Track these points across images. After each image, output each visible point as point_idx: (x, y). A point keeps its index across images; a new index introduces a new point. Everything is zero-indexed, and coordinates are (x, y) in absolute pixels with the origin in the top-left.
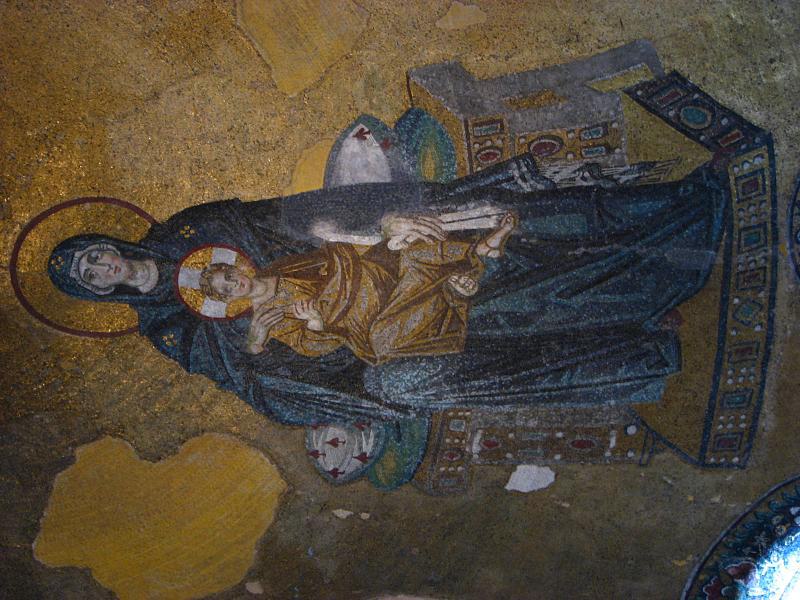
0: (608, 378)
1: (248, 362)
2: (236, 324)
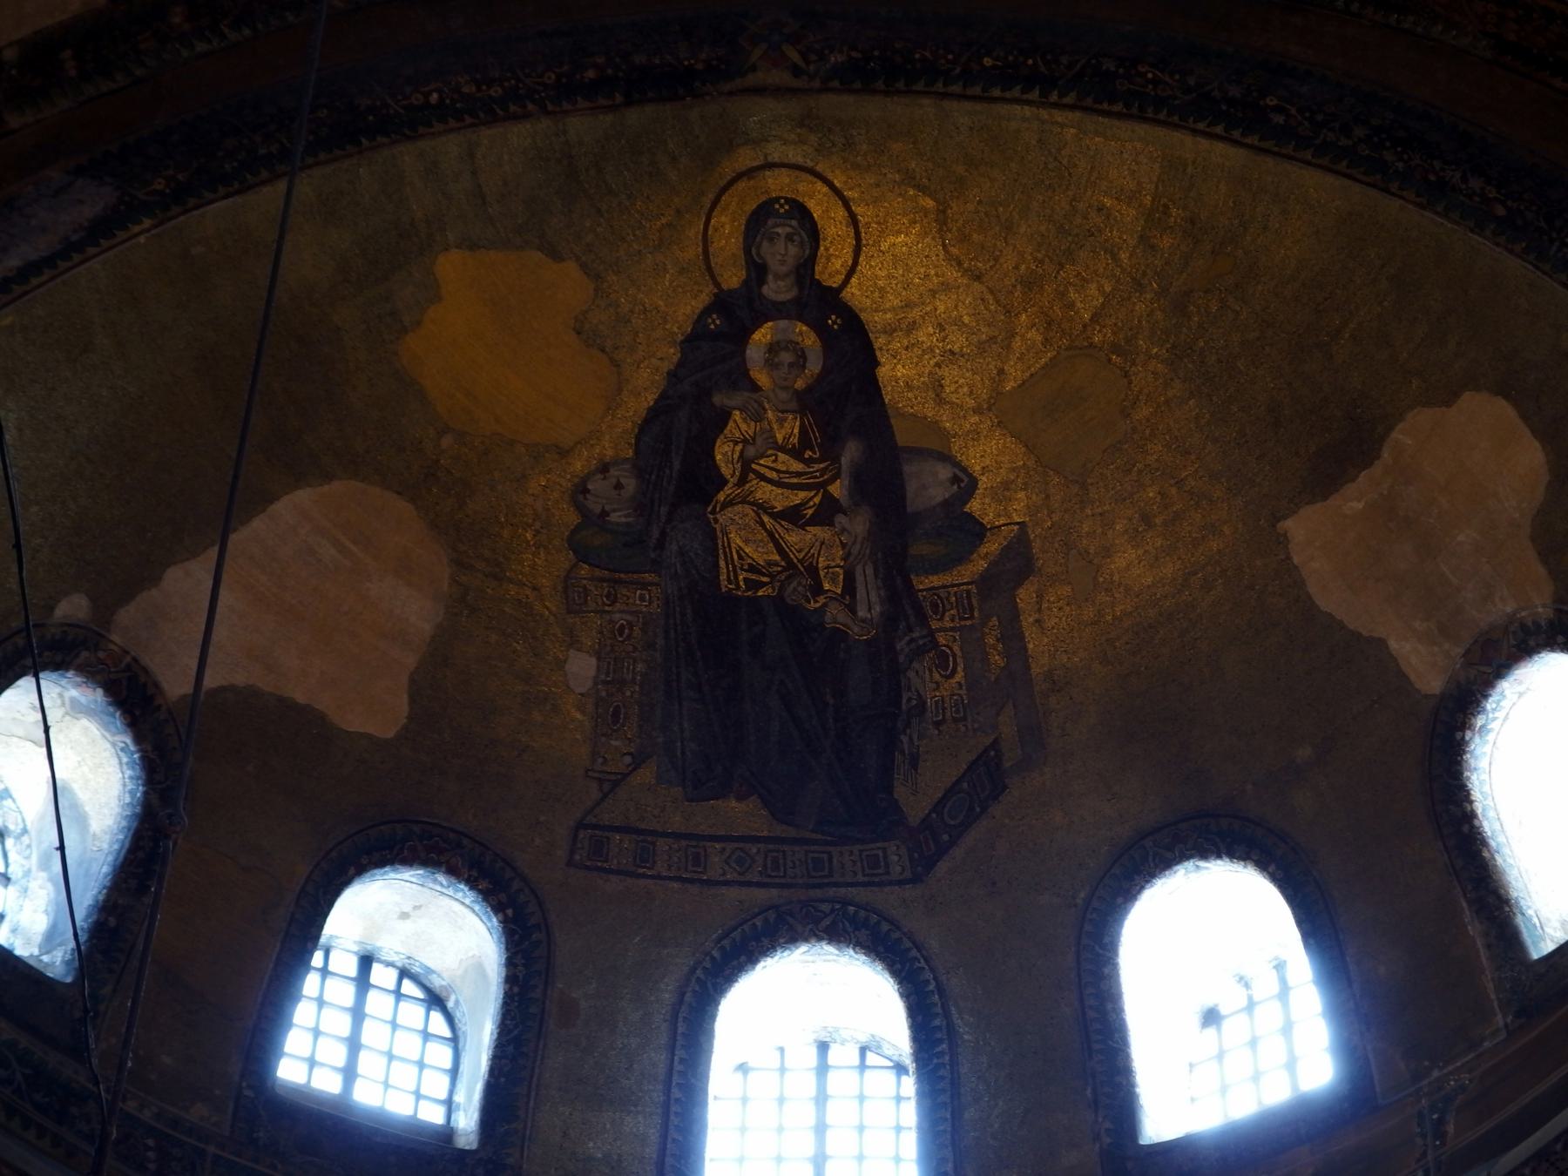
2: (741, 379)
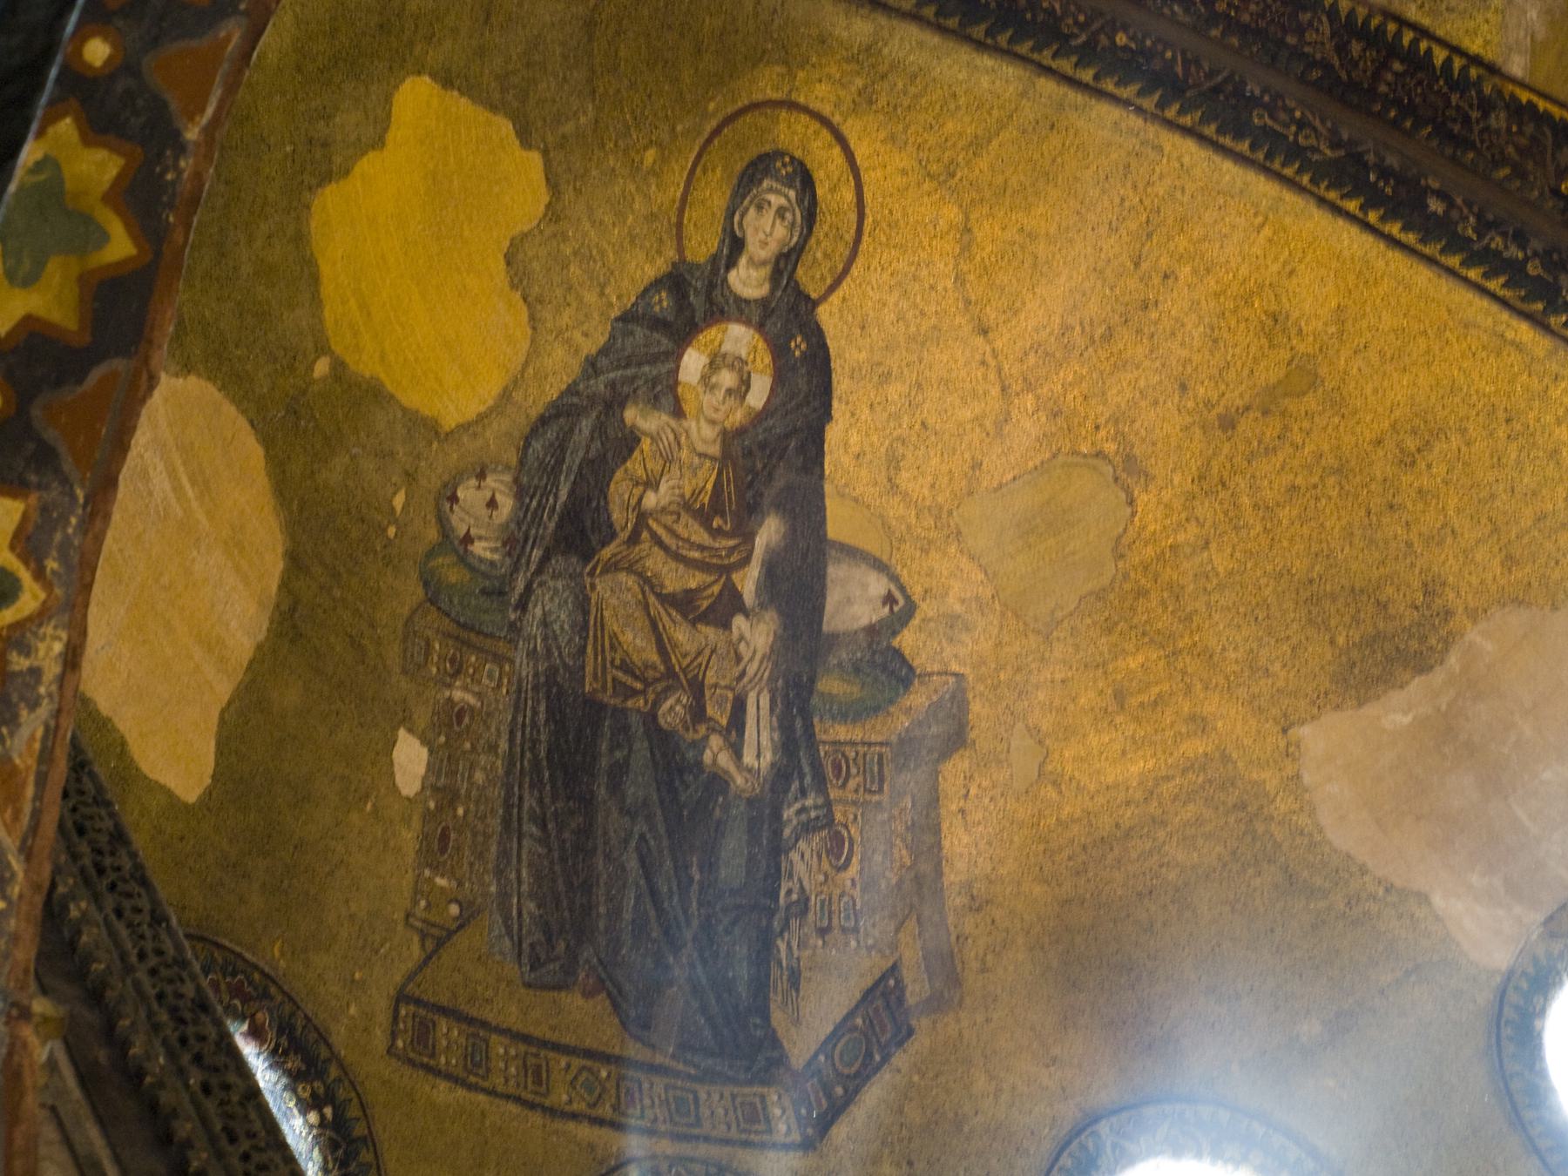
0: (525, 888)
1: (614, 403)
2: (666, 395)
